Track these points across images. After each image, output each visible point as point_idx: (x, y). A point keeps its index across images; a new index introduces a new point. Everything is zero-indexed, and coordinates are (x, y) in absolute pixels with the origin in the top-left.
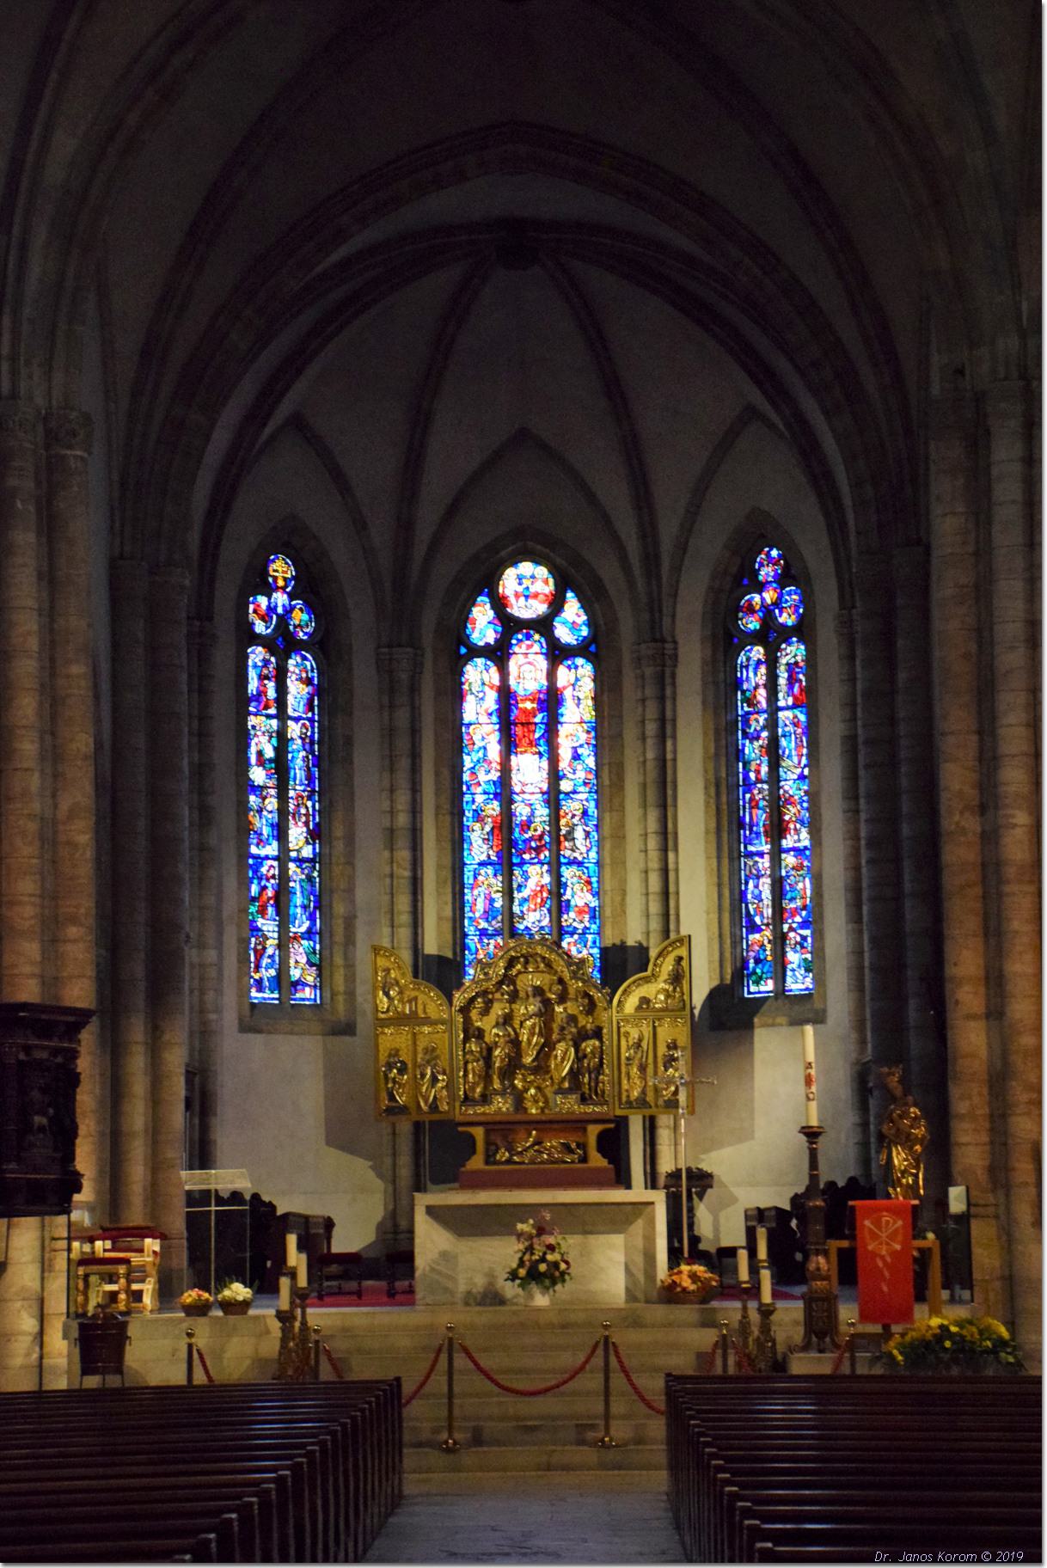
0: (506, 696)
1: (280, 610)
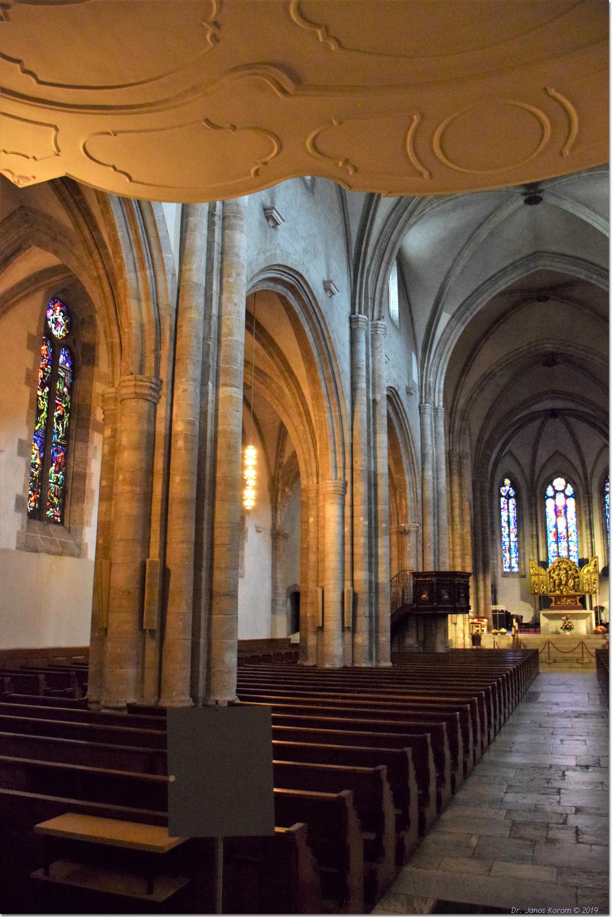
0: (556, 506)
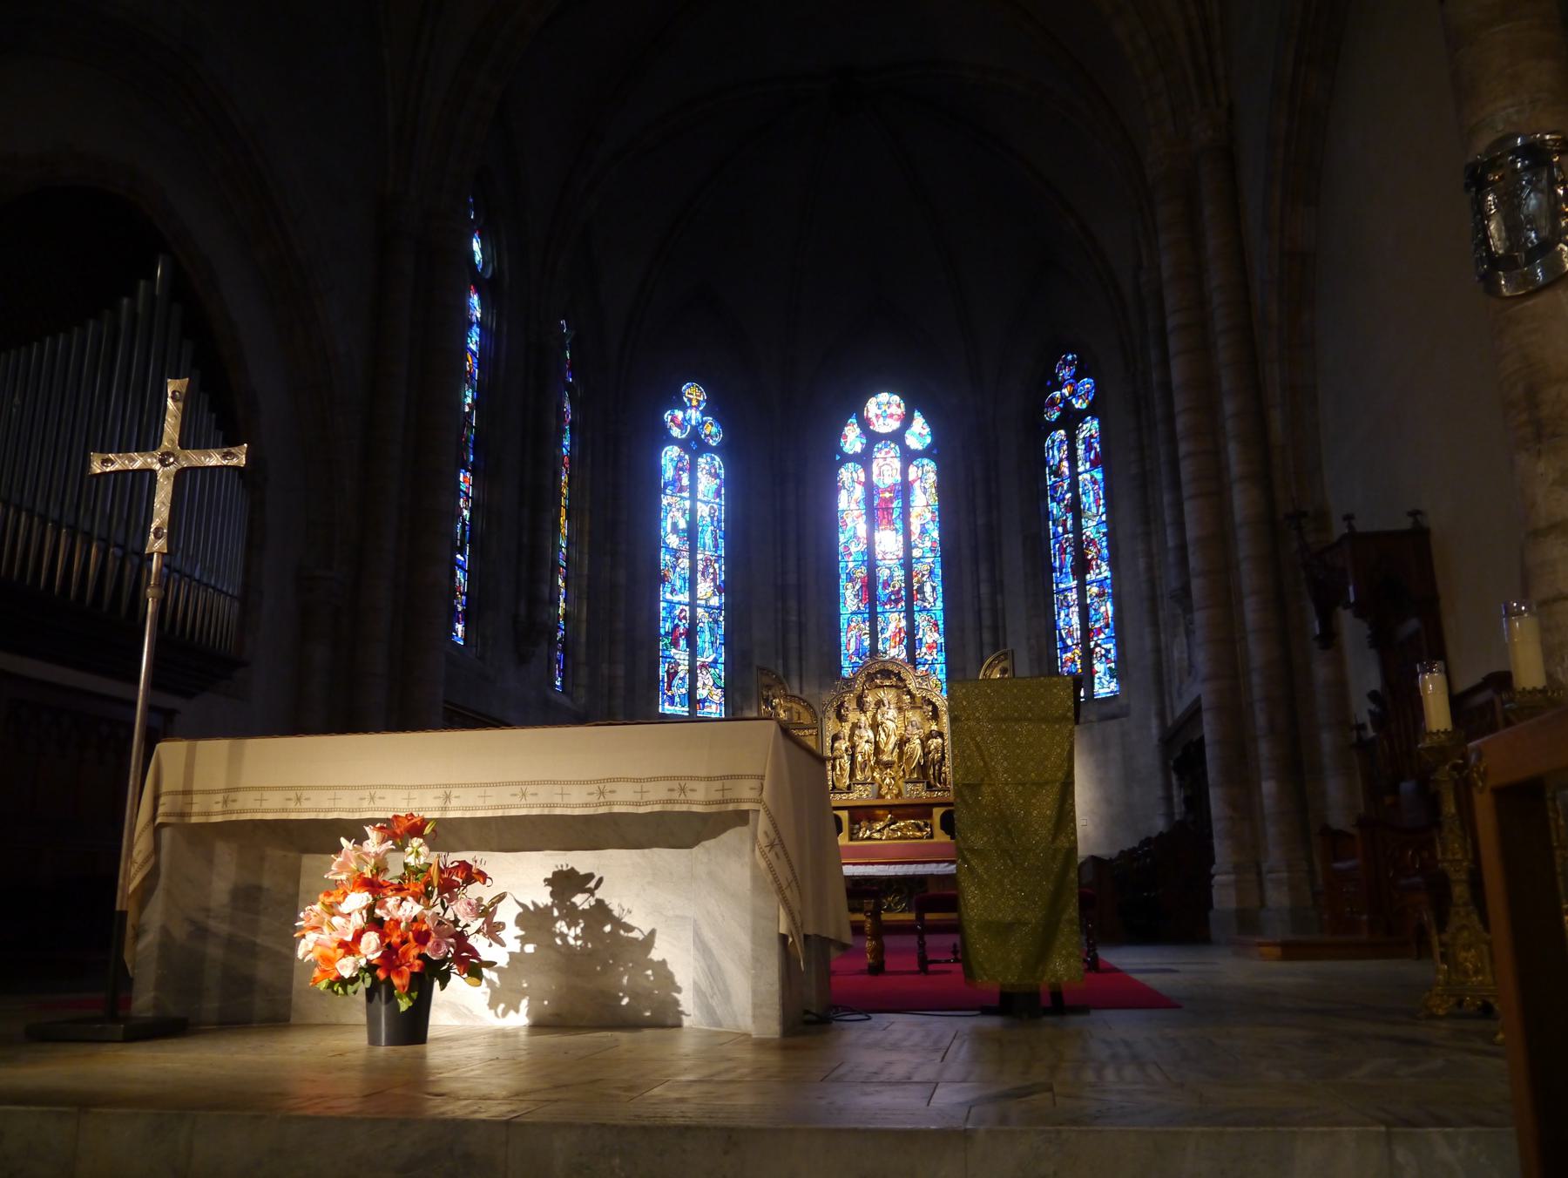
0: (870, 487)
1: (693, 423)
